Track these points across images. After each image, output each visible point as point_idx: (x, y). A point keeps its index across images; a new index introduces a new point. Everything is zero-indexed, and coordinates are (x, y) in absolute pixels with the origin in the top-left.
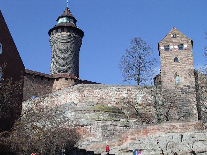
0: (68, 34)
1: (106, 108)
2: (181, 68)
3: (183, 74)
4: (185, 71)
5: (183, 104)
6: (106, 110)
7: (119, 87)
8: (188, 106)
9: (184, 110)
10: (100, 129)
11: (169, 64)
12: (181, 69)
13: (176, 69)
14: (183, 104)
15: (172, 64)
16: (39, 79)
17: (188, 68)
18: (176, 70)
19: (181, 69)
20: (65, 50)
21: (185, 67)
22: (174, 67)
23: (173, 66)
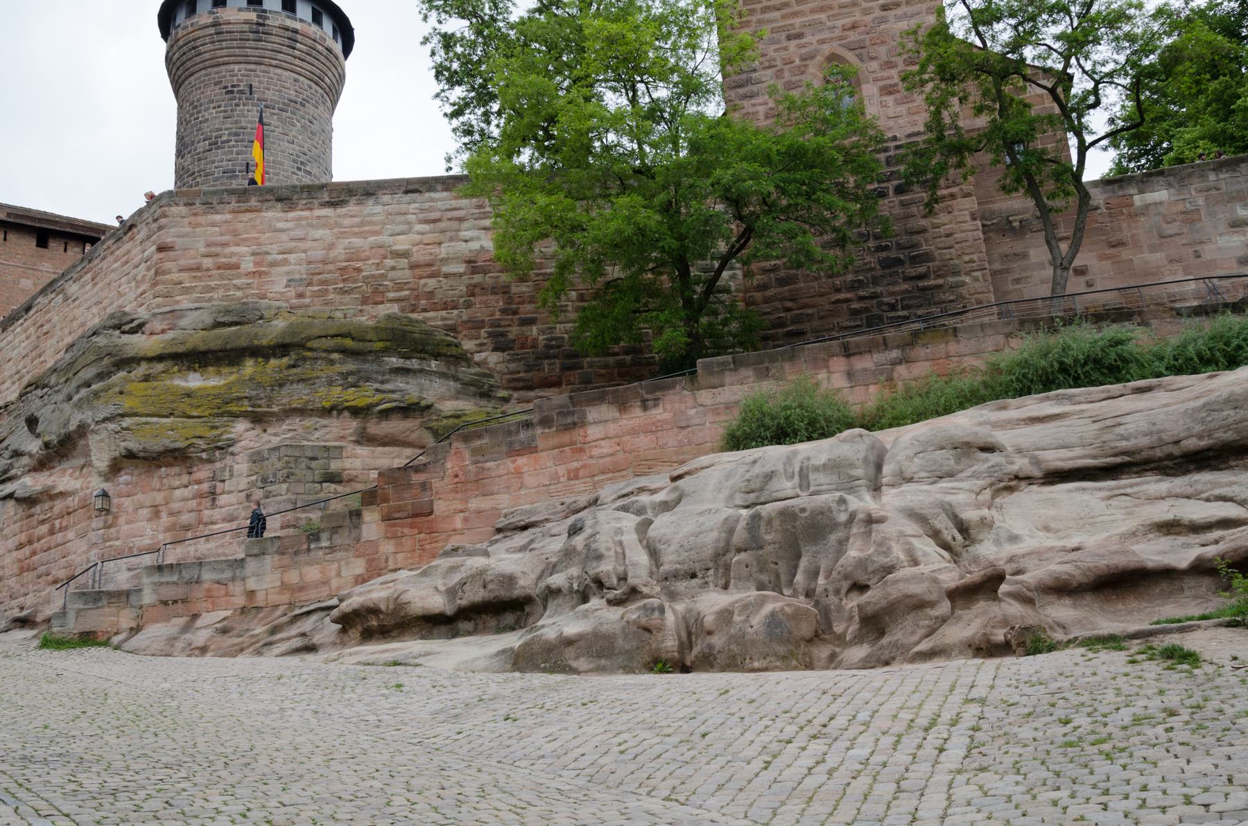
0: (252, 16)
1: (331, 332)
2: (854, 27)
3: (874, 65)
4: (883, 42)
5: (883, 268)
6: (330, 343)
7: (435, 190)
8: (921, 277)
9: (893, 307)
10: (275, 475)
11: (777, 14)
12: (853, 36)
13: (822, 42)
14: (888, 264)
15: (795, 14)
16: (65, 250)
17: (904, 25)
18: (827, 49)
19: (853, 36)
20: (237, 105)
21: (883, 20)
22: (806, 30)
23: (797, 21)
